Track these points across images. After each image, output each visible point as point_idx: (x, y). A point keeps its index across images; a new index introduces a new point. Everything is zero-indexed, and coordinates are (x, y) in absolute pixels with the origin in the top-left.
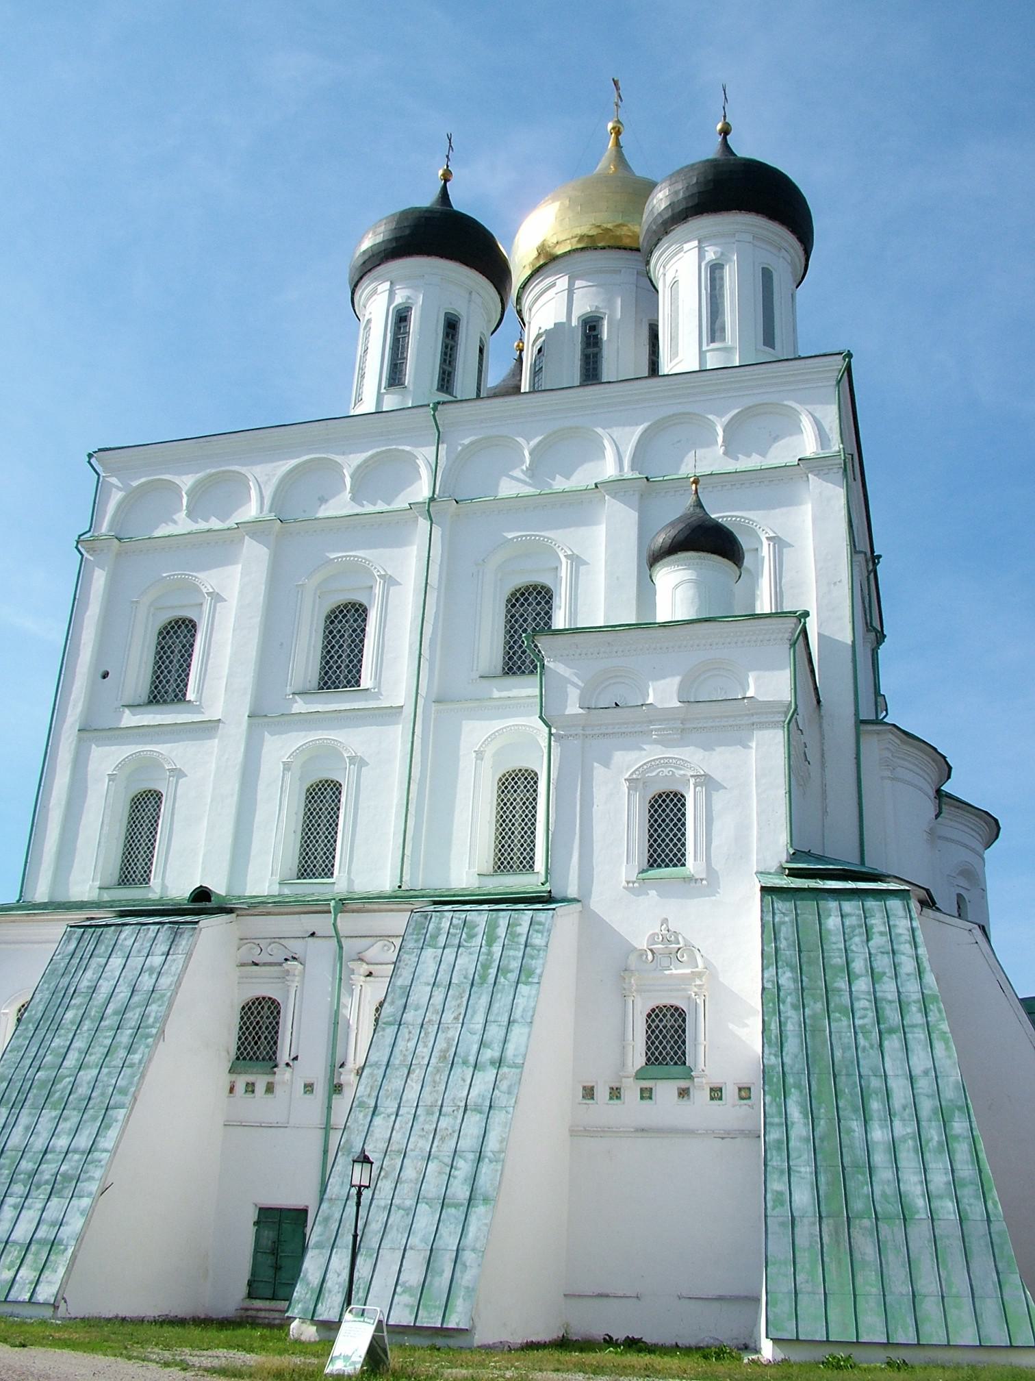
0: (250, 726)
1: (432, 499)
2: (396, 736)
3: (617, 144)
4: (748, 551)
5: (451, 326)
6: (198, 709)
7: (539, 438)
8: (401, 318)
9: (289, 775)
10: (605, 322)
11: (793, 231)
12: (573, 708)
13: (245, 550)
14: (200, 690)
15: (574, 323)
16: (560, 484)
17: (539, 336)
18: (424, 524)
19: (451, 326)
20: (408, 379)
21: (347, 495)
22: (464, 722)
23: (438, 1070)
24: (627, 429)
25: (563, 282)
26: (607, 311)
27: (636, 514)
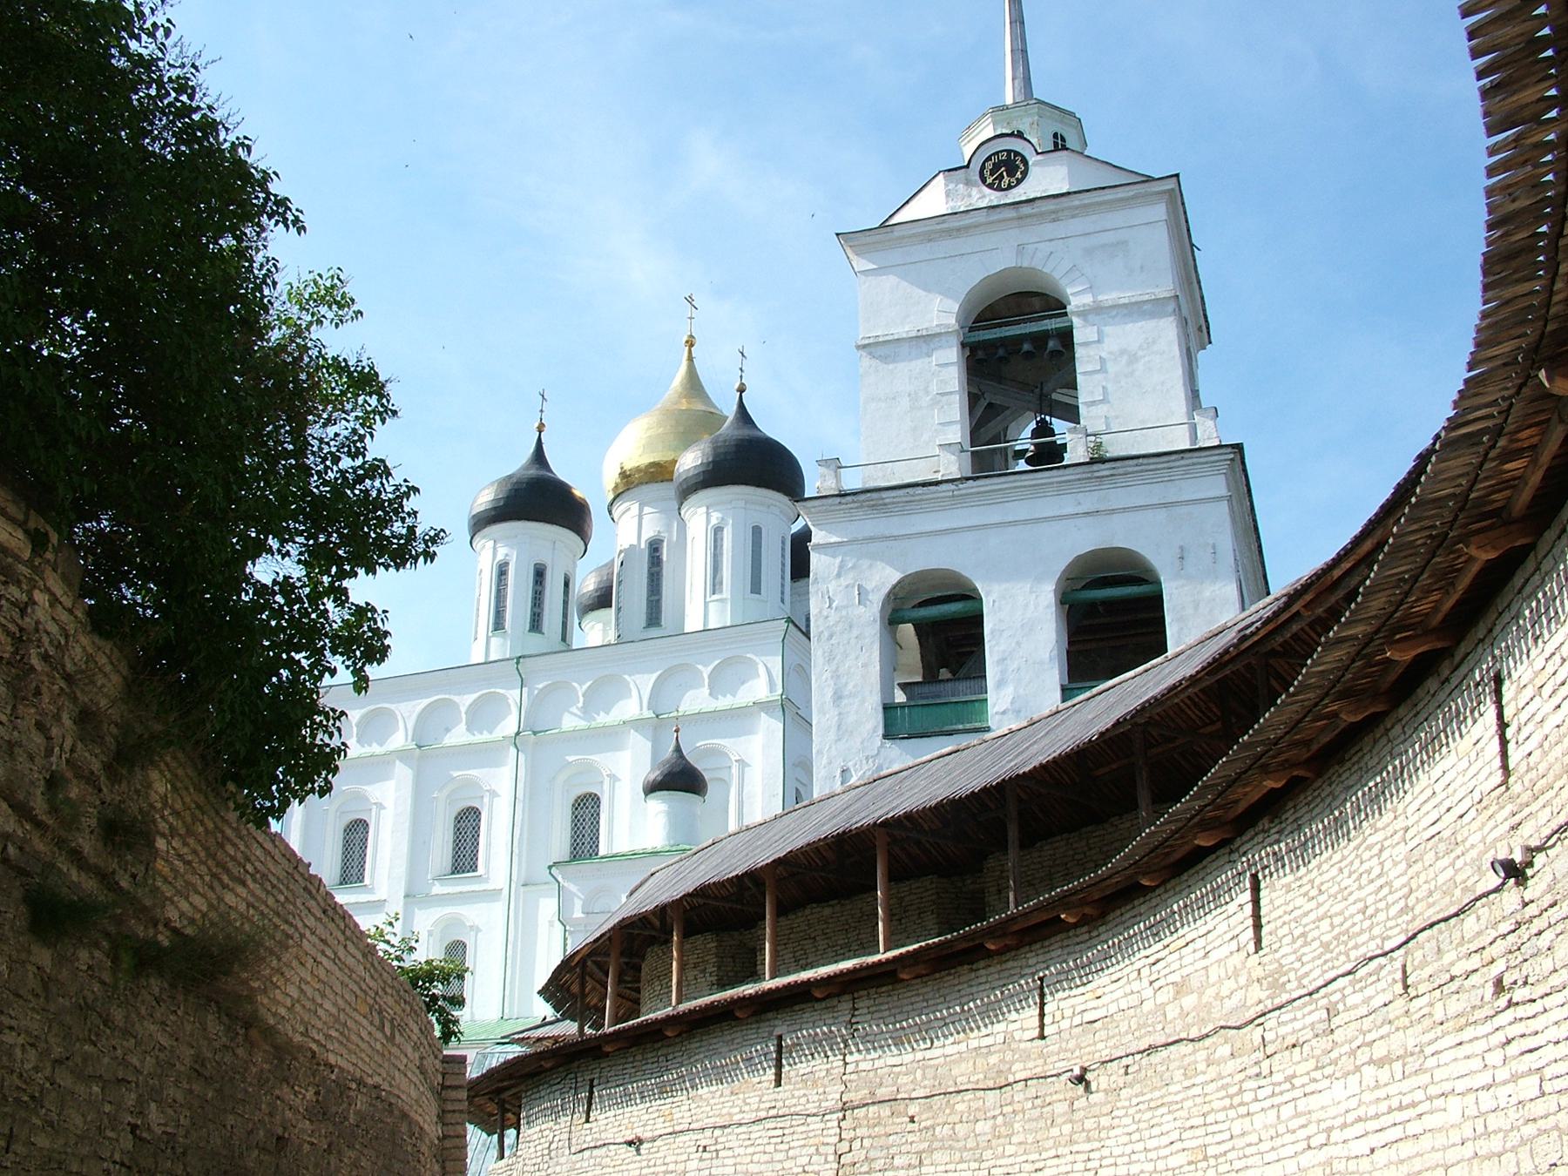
0: (405, 904)
1: (518, 734)
2: (499, 908)
3: (690, 359)
4: (711, 779)
5: (540, 574)
6: (371, 891)
7: (589, 683)
8: (502, 571)
9: (431, 939)
10: (665, 544)
11: (778, 490)
12: (578, 914)
13: (397, 770)
14: (372, 877)
15: (643, 546)
16: (602, 719)
17: (621, 552)
18: (513, 750)
19: (540, 574)
20: (508, 625)
21: (463, 726)
22: (541, 900)
23: (481, 1152)
24: (646, 676)
25: (635, 508)
26: (666, 535)
27: (649, 744)
